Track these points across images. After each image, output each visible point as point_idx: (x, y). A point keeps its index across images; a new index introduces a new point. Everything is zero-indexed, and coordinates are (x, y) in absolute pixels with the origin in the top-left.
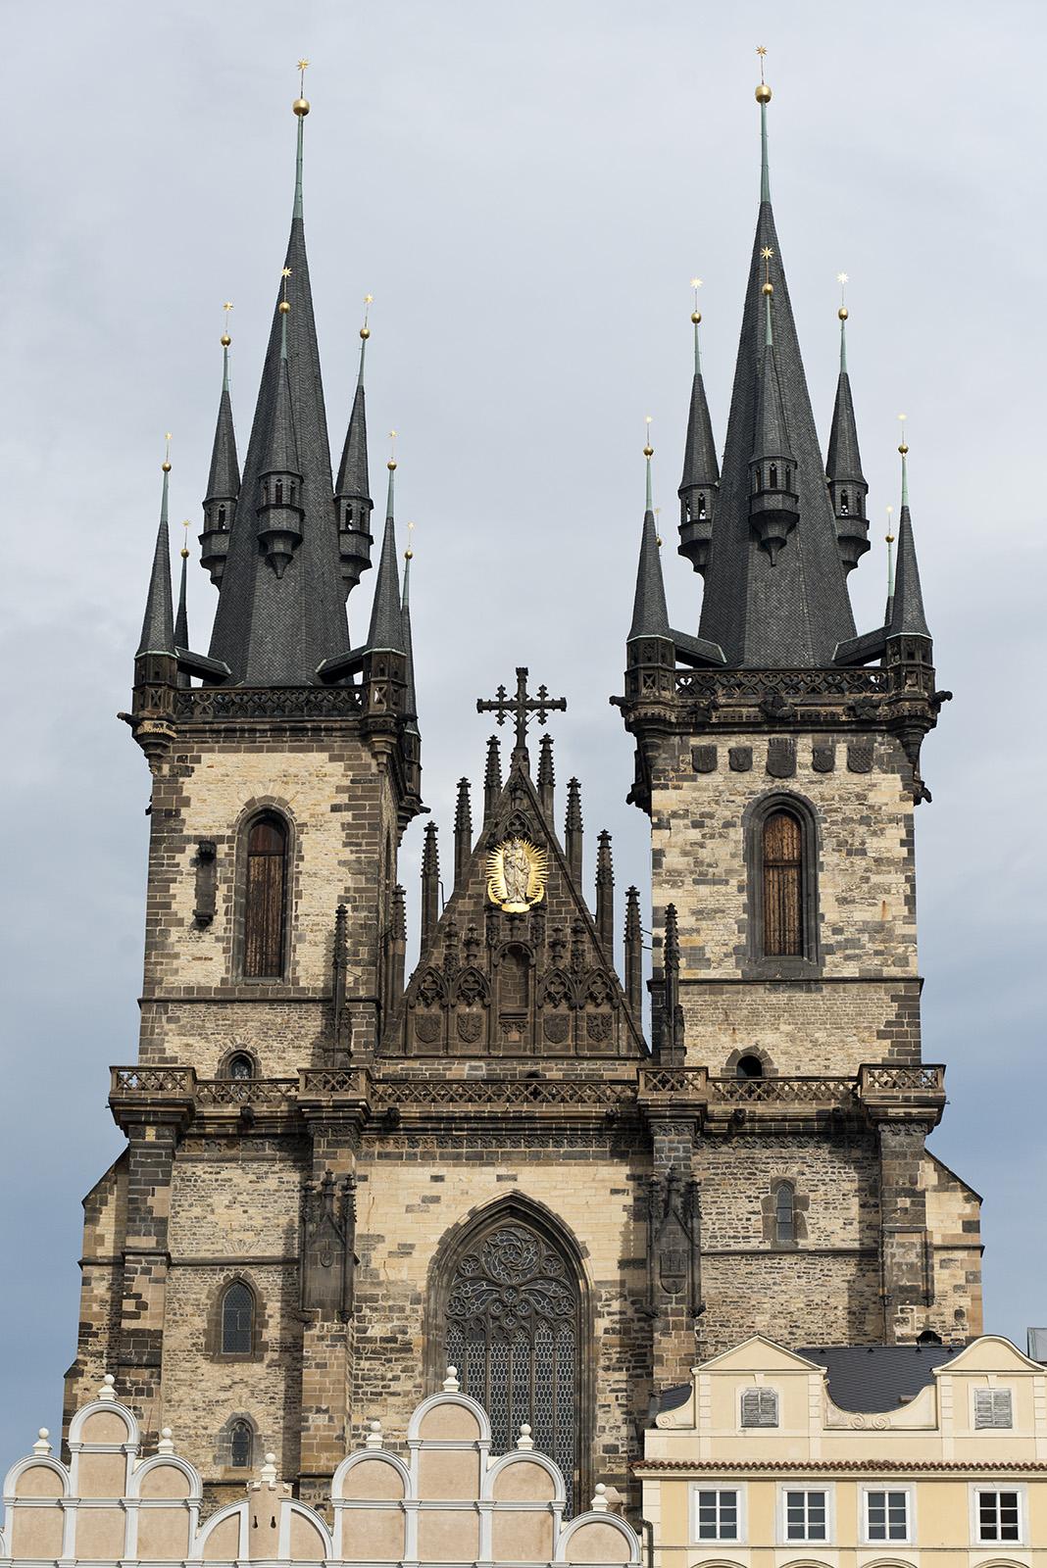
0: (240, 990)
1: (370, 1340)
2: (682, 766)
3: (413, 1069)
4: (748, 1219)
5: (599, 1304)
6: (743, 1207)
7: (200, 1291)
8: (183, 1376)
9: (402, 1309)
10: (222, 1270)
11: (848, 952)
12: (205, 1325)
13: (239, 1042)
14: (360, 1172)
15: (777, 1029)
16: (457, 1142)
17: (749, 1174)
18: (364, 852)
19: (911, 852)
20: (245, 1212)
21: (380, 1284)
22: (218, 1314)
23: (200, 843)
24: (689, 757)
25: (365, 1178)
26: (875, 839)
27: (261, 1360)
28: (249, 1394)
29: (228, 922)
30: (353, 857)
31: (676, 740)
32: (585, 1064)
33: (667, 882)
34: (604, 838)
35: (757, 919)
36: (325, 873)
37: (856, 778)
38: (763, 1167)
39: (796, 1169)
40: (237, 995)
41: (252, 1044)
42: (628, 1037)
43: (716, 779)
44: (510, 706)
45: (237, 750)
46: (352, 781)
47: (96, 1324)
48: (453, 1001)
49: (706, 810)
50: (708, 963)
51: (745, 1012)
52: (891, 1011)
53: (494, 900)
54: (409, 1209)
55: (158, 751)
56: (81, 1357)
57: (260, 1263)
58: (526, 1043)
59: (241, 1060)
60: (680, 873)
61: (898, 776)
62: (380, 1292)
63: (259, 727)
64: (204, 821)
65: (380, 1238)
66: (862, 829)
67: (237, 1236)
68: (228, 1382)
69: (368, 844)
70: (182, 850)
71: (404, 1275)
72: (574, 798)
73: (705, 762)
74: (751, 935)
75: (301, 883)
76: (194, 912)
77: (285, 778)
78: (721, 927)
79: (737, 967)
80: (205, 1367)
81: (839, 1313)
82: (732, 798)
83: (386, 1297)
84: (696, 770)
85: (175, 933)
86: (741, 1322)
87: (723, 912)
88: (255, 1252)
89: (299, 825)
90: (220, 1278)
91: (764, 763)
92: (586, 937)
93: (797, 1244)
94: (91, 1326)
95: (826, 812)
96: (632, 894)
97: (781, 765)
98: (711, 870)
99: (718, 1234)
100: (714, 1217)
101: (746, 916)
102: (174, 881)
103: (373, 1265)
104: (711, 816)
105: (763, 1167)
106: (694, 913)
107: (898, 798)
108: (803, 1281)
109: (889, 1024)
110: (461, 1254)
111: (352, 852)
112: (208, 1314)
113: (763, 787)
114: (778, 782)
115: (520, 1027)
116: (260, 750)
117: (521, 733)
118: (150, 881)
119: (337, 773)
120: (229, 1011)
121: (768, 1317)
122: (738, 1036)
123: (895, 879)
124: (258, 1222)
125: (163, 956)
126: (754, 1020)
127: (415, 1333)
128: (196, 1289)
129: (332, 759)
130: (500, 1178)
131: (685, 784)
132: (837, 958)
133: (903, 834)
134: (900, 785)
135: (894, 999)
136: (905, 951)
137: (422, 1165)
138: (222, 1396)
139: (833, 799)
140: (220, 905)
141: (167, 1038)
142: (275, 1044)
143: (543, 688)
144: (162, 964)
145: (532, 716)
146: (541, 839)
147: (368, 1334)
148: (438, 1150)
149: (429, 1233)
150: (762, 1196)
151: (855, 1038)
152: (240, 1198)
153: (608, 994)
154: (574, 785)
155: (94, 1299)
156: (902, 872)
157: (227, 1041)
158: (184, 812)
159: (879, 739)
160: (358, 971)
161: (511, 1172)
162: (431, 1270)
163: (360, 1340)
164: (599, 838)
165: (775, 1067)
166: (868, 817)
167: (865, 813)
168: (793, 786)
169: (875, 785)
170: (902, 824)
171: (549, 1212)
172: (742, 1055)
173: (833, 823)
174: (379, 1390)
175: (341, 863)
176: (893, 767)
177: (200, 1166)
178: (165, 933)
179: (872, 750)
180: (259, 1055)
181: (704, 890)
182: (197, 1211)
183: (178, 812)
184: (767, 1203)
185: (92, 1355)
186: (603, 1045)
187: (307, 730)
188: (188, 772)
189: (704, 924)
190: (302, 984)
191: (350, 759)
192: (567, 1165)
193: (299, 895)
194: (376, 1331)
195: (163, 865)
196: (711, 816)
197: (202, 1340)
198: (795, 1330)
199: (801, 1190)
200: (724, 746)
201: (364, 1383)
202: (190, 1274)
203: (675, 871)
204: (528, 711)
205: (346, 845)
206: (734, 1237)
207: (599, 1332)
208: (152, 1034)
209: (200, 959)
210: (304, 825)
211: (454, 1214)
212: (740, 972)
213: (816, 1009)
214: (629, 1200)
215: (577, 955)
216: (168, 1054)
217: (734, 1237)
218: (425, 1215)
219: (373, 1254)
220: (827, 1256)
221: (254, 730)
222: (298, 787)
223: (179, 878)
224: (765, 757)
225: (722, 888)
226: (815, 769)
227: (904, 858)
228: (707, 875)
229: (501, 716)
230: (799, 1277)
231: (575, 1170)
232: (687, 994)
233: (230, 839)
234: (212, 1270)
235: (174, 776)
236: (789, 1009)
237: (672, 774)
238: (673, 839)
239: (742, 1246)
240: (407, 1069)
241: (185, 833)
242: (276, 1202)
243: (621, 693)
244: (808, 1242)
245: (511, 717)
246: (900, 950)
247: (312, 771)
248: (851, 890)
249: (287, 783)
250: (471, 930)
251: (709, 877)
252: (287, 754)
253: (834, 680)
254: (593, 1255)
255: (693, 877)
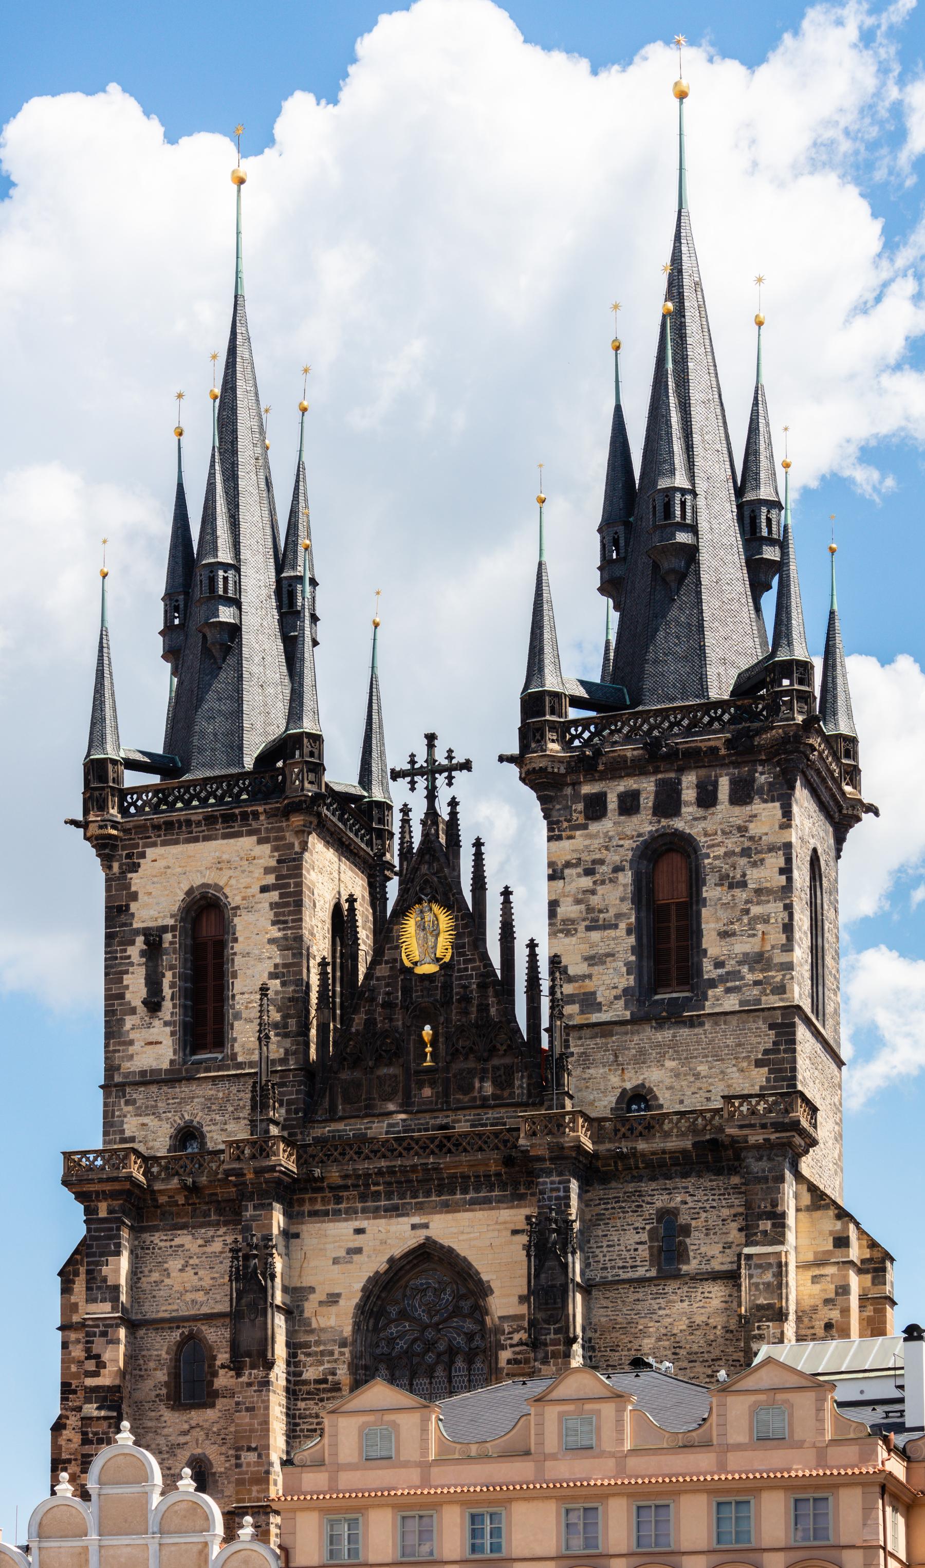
0: (186, 1070)
1: (306, 1382)
2: (575, 816)
3: (338, 1131)
4: (636, 1250)
5: (502, 1338)
6: (631, 1238)
7: (161, 1346)
8: (150, 1424)
9: (331, 1353)
10: (178, 1327)
11: (729, 984)
12: (166, 1378)
13: (187, 1117)
14: (294, 1229)
15: (663, 1065)
16: (376, 1196)
17: (638, 1206)
18: (290, 928)
19: (790, 880)
20: (196, 1274)
21: (312, 1331)
22: (177, 1367)
23: (145, 935)
24: (580, 807)
25: (297, 1236)
26: (755, 871)
27: (213, 1406)
28: (204, 1437)
29: (174, 1006)
30: (280, 934)
31: (569, 791)
32: (491, 1114)
33: (561, 931)
34: (507, 893)
35: (645, 959)
36: (257, 952)
37: (737, 810)
38: (648, 1199)
39: (679, 1199)
40: (184, 1074)
41: (198, 1119)
42: (528, 1085)
43: (606, 825)
44: (421, 772)
45: (176, 842)
46: (279, 862)
47: (74, 1383)
48: (370, 1063)
49: (598, 856)
50: (598, 1007)
51: (634, 1051)
52: (768, 1039)
53: (407, 964)
54: (336, 1261)
55: (107, 851)
56: (65, 1412)
57: (209, 1318)
58: (438, 1097)
59: (187, 1135)
60: (573, 922)
61: (777, 804)
62: (312, 1338)
63: (193, 818)
64: (153, 913)
65: (312, 1290)
66: (743, 861)
67: (189, 1297)
68: (186, 1427)
69: (293, 921)
70: (132, 943)
71: (332, 1322)
72: (479, 858)
73: (596, 808)
74: (639, 979)
75: (236, 963)
76: (145, 1002)
77: (220, 864)
78: (612, 971)
79: (626, 1008)
80: (168, 1415)
81: (718, 1333)
82: (621, 842)
83: (318, 1343)
84: (587, 818)
85: (130, 1022)
86: (629, 1345)
87: (613, 955)
88: (205, 1310)
89: (233, 909)
90: (176, 1335)
91: (650, 804)
92: (491, 992)
93: (680, 1270)
94: (70, 1384)
95: (709, 847)
96: (532, 945)
97: (669, 803)
98: (601, 916)
99: (609, 1265)
100: (605, 1250)
101: (633, 958)
102: (127, 972)
103: (307, 1314)
104: (602, 862)
105: (648, 1199)
106: (586, 959)
107: (777, 827)
108: (687, 1303)
109: (766, 1052)
110: (385, 1294)
111: (280, 930)
112: (168, 1368)
113: (650, 828)
114: (664, 822)
115: (432, 1084)
116: (196, 840)
117: (431, 796)
118: (106, 974)
119: (265, 855)
120: (178, 1090)
121: (653, 1340)
122: (627, 1075)
123: (774, 909)
124: (207, 1283)
125: (120, 1044)
126: (641, 1059)
127: (343, 1374)
128: (157, 1346)
129: (260, 842)
130: (414, 1227)
131: (578, 833)
132: (720, 990)
133: (781, 862)
134: (779, 813)
135: (771, 1027)
136: (782, 980)
137: (346, 1220)
138: (182, 1439)
139: (716, 834)
140: (167, 992)
141: (126, 1120)
142: (218, 1117)
143: (450, 751)
144: (119, 1051)
145: (441, 779)
146: (448, 896)
147: (305, 1376)
148: (360, 1205)
149: (352, 1283)
150: (648, 1227)
151: (735, 1069)
152: (191, 1262)
153: (509, 1046)
154: (478, 844)
155: (73, 1360)
156: (781, 900)
157: (177, 1118)
158: (133, 907)
159: (760, 769)
160: (288, 1043)
161: (424, 1220)
162: (355, 1316)
163: (297, 1383)
164: (502, 894)
165: (661, 1101)
166: (749, 848)
167: (747, 844)
168: (679, 824)
169: (755, 816)
170: (781, 852)
171: (458, 1255)
172: (630, 1094)
173: (716, 858)
174: (314, 1427)
175: (271, 941)
176: (773, 797)
177: (157, 1234)
178: (121, 1022)
179: (754, 780)
180: (205, 1129)
181: (595, 936)
182: (155, 1276)
183: (128, 906)
184: (653, 1234)
185: (73, 1409)
186: (506, 1094)
187: (234, 815)
188: (135, 868)
189: (596, 970)
190: (240, 1059)
191: (277, 839)
192: (472, 1210)
193: (235, 975)
194: (311, 1373)
195: (116, 958)
196: (602, 862)
197: (164, 1391)
198: (678, 1350)
199: (683, 1219)
200: (614, 791)
201: (301, 1421)
202: (152, 1334)
203: (568, 920)
204: (437, 775)
205: (274, 923)
206: (623, 1267)
207: (502, 1363)
208: (113, 1116)
209: (151, 1043)
210: (238, 908)
211: (373, 1263)
212: (628, 1013)
213: (698, 1042)
214: (524, 1239)
215: (483, 1008)
216: (128, 1134)
217: (623, 1267)
218: (349, 1266)
219: (307, 1305)
220: (707, 1280)
221: (189, 823)
222: (231, 873)
223: (131, 969)
224: (652, 798)
225: (612, 933)
226: (699, 806)
227: (783, 887)
228: (597, 921)
229: (413, 783)
230: (682, 1301)
231: (480, 1215)
232: (580, 1038)
233: (173, 928)
234: (170, 1328)
235: (123, 873)
236: (673, 1045)
237: (565, 824)
238: (568, 889)
239: (630, 1275)
240: (333, 1131)
241: (135, 926)
242: (221, 1263)
243: (515, 750)
244: (691, 1267)
245: (421, 783)
246: (778, 979)
247: (242, 854)
248: (732, 923)
249: (221, 869)
250: (388, 994)
251: (601, 922)
252: (220, 842)
253: (716, 713)
254: (497, 1292)
255: (587, 923)
